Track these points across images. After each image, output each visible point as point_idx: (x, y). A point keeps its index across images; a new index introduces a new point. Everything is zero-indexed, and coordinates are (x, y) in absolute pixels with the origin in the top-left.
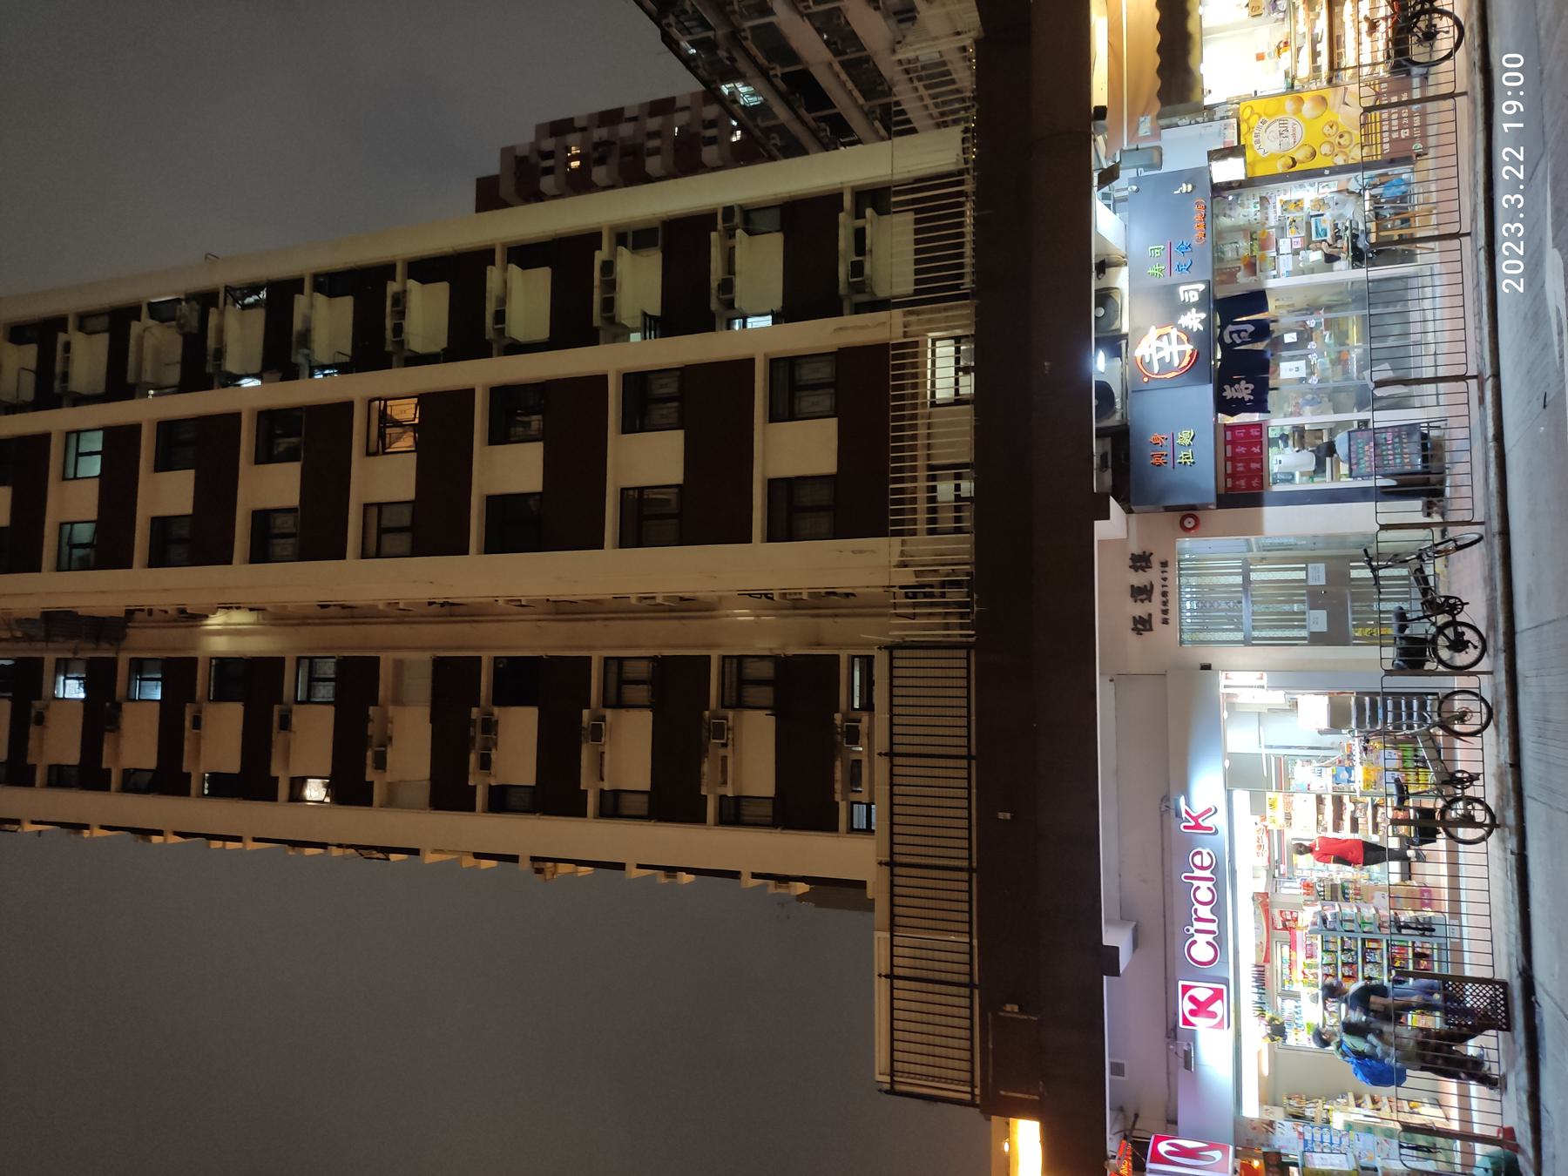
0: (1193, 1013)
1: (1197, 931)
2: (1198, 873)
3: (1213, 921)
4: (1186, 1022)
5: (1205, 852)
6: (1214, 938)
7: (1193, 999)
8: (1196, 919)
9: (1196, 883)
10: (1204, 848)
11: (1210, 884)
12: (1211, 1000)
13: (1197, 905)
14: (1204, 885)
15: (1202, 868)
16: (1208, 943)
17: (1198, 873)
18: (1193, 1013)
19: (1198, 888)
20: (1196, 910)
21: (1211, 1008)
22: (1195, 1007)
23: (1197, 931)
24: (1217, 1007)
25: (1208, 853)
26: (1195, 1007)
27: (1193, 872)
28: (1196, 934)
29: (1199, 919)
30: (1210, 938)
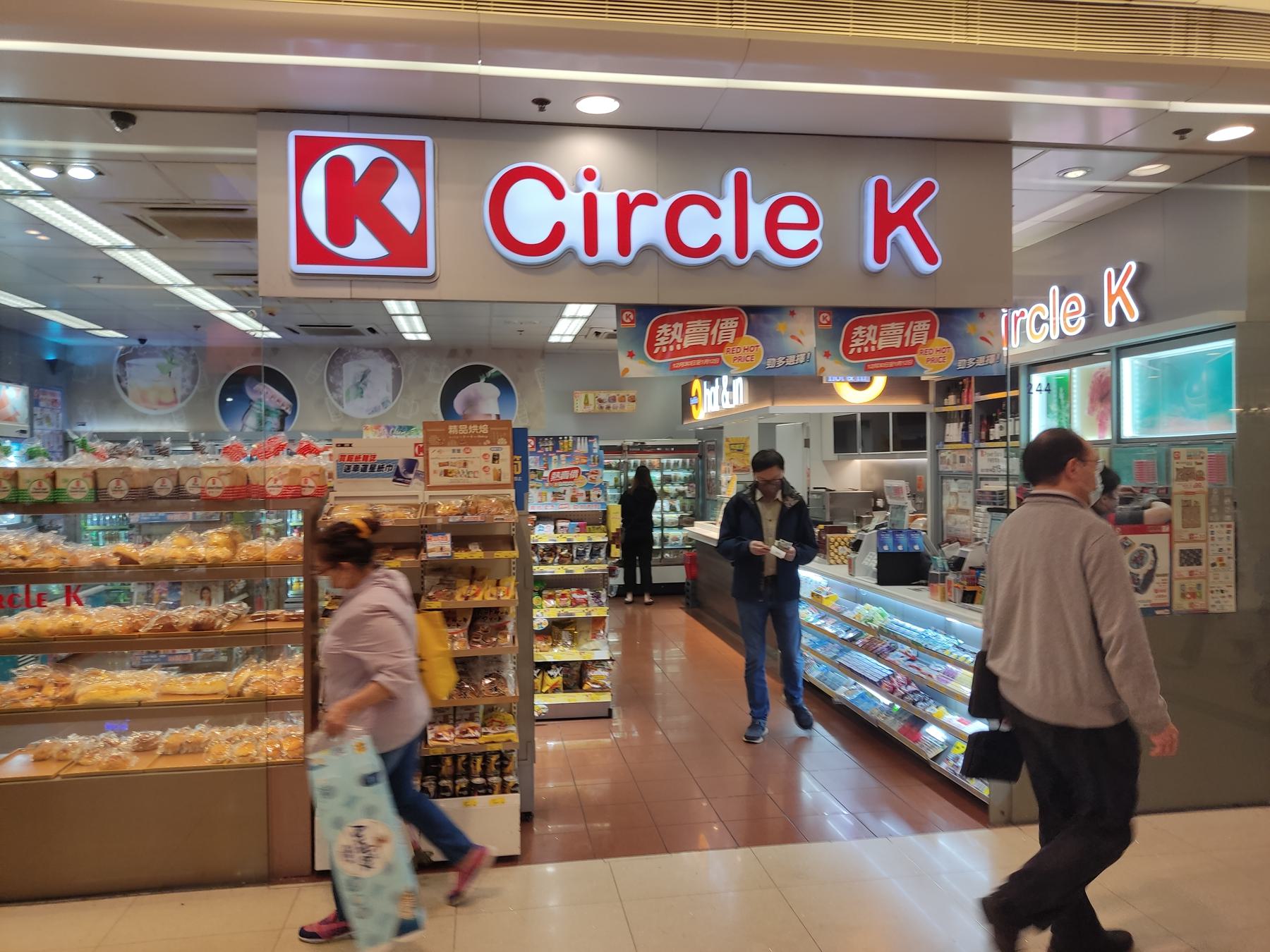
0: (339, 169)
1: (590, 203)
2: (757, 215)
3: (624, 246)
4: (308, 153)
5: (814, 235)
6: (571, 251)
7: (381, 174)
8: (622, 199)
9: (728, 206)
10: (822, 235)
11: (728, 246)
12: (385, 227)
13: (664, 205)
14: (726, 227)
15: (772, 226)
16: (559, 230)
17: (757, 215)
18: (339, 169)
19: (715, 212)
20: (649, 200)
21: (360, 228)
22: (358, 174)
23: (590, 203)
24: (366, 245)
25: (813, 245)
26: (358, 175)
27: (759, 201)
28: (581, 196)
29: (625, 208)
30: (575, 236)
